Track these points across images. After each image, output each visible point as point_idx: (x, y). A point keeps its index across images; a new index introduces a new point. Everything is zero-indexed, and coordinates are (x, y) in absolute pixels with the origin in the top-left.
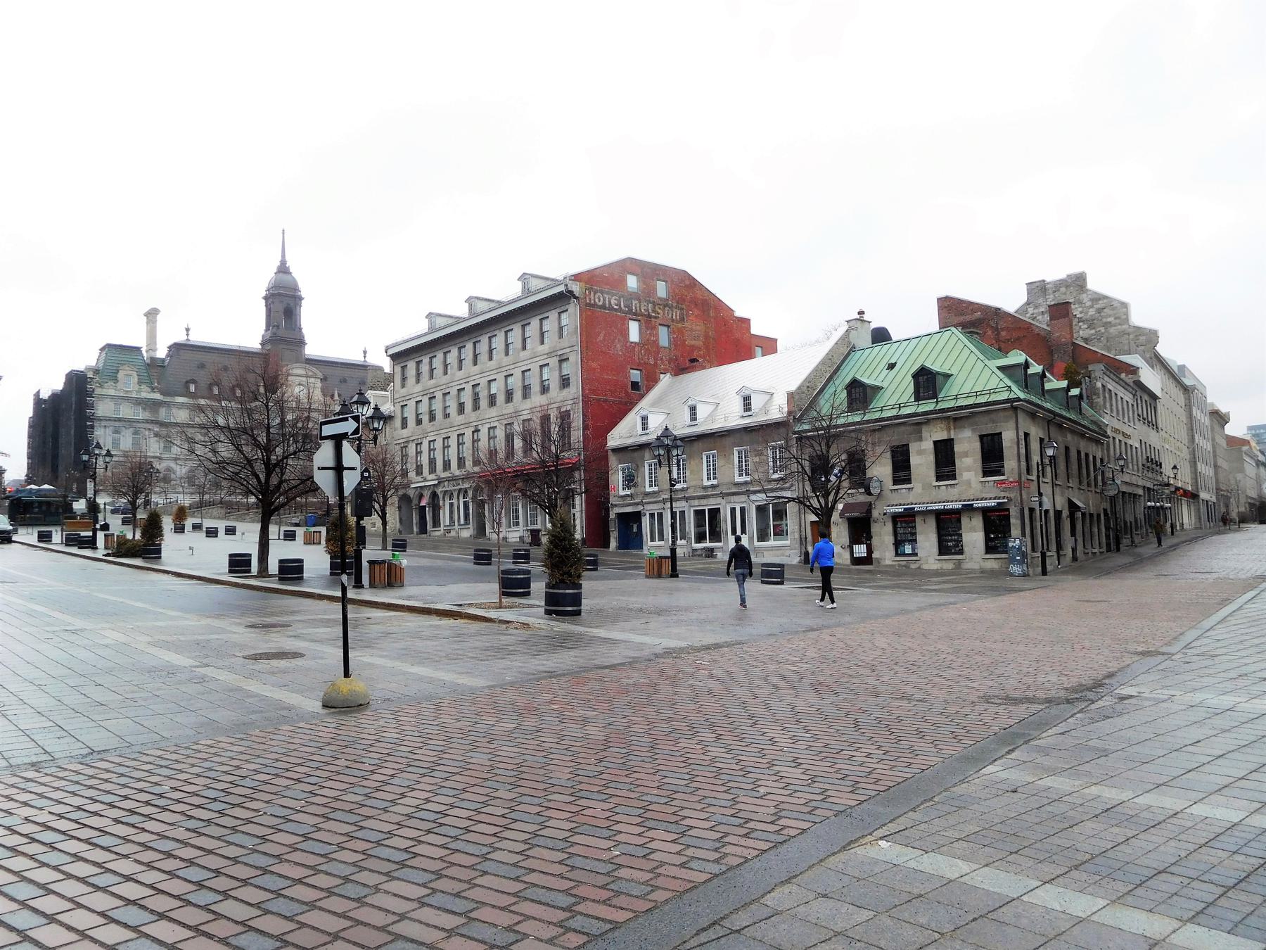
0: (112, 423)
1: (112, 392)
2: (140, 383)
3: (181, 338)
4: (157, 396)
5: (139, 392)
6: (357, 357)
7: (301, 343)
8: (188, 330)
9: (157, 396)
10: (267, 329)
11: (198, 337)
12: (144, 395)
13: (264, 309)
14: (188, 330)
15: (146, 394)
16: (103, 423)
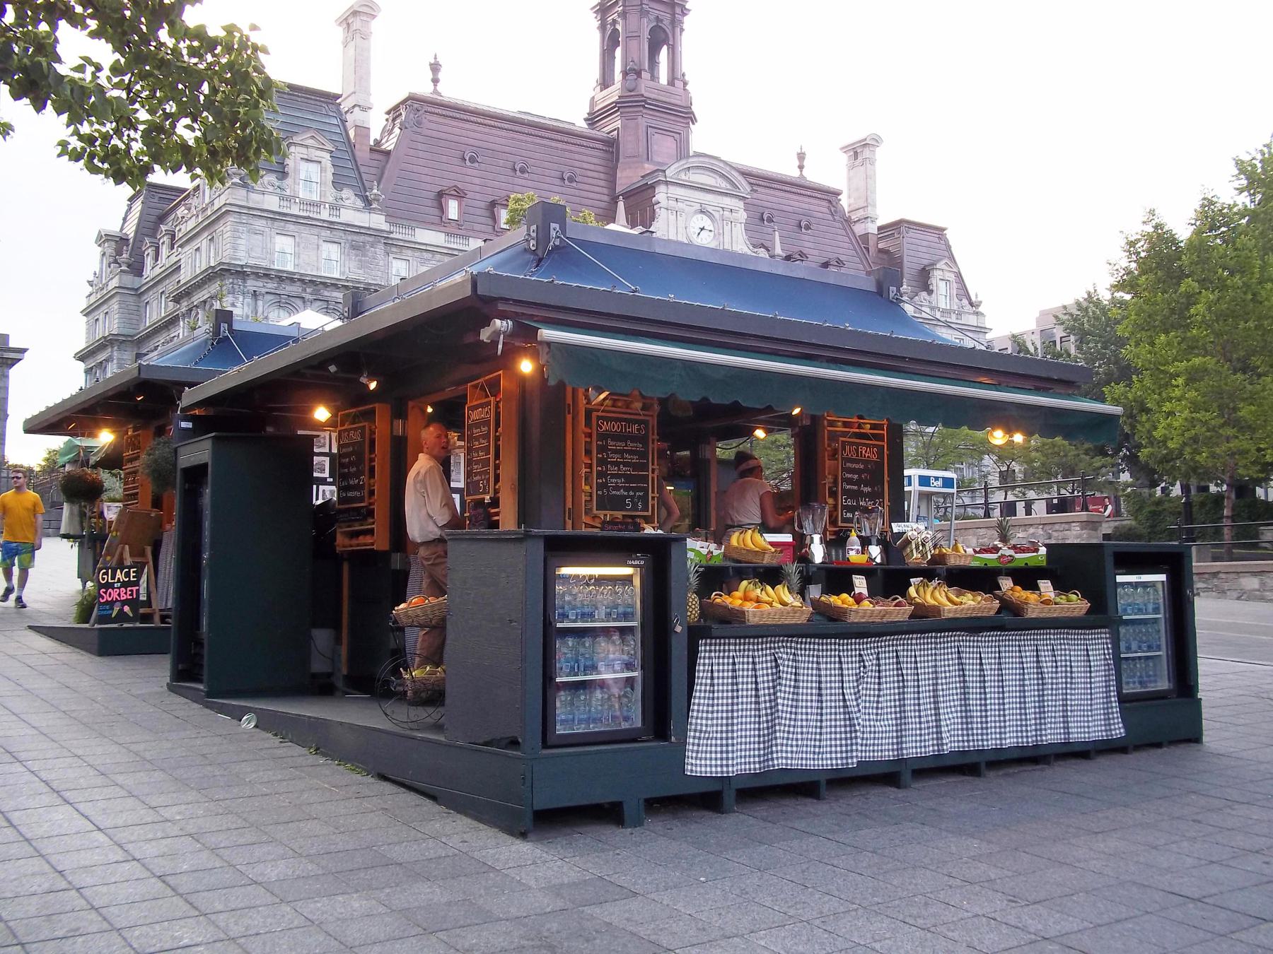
0: (271, 285)
1: (272, 203)
2: (338, 184)
3: (424, 88)
4: (377, 221)
5: (335, 207)
6: (789, 170)
7: (687, 116)
8: (435, 67)
9: (377, 221)
10: (605, 83)
11: (454, 90)
12: (347, 216)
13: (597, 36)
14: (435, 67)
15: (352, 215)
16: (252, 284)
